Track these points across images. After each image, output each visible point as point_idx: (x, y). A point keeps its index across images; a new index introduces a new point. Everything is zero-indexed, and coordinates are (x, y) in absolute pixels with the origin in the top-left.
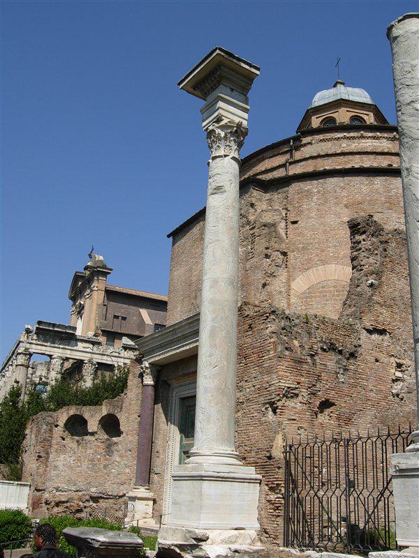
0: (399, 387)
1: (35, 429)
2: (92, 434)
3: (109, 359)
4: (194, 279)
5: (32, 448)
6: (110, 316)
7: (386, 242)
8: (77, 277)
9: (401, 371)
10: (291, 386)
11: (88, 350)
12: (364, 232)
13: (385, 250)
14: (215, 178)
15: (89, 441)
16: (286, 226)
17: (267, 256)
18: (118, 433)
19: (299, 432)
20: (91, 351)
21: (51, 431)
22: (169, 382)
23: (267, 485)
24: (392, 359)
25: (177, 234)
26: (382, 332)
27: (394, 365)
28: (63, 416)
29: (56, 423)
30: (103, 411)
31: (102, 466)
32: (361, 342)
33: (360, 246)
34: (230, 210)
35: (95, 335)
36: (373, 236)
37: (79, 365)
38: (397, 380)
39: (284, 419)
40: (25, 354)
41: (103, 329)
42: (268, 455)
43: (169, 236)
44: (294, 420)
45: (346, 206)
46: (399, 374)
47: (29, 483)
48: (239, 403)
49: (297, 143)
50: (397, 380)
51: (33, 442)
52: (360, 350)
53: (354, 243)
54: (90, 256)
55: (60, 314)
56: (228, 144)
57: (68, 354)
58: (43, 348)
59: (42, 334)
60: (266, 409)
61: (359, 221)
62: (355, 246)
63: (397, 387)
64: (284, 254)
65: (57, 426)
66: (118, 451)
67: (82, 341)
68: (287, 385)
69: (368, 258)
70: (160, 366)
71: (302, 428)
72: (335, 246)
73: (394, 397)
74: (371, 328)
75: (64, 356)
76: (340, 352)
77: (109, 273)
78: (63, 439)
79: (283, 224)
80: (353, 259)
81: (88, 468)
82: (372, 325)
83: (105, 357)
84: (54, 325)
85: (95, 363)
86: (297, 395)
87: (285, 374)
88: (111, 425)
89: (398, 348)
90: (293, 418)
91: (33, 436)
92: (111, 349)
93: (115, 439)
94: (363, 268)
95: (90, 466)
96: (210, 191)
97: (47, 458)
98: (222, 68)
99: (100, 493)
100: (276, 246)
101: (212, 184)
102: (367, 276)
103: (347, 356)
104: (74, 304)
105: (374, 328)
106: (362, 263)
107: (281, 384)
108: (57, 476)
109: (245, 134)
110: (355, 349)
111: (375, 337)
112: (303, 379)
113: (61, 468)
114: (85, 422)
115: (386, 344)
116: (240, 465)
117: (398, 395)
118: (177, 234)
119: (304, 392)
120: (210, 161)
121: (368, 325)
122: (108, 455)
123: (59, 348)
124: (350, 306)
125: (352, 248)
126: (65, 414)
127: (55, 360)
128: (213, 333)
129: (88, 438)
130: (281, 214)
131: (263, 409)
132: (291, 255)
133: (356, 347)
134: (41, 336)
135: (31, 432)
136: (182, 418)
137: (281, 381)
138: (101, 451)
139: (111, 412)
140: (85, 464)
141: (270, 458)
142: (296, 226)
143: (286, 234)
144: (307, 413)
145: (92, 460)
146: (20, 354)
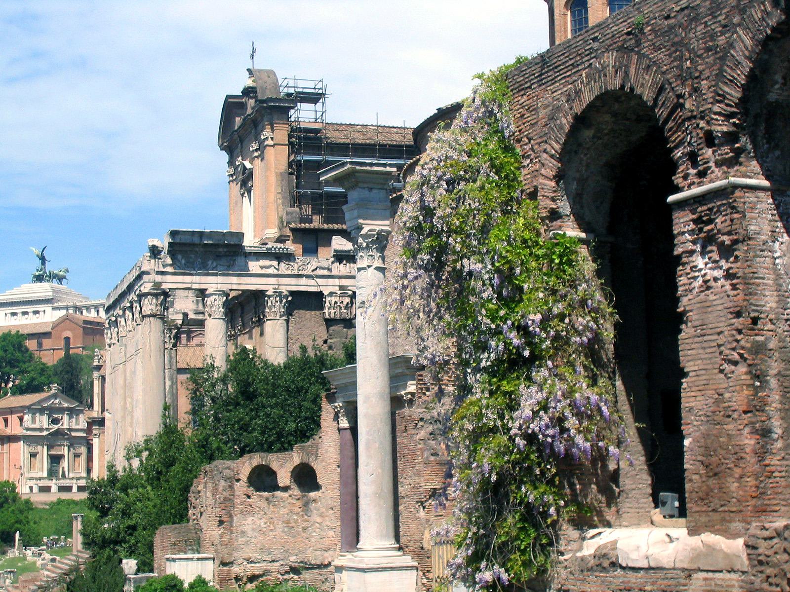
1: (210, 485)
2: (286, 489)
3: (311, 282)
5: (209, 509)
8: (231, 107)
11: (271, 271)
15: (282, 499)
18: (317, 487)
20: (276, 272)
21: (231, 487)
23: (421, 570)
28: (245, 466)
29: (237, 477)
30: (295, 459)
31: (301, 529)
34: (377, 325)
40: (156, 296)
41: (293, 226)
47: (212, 556)
51: (210, 501)
56: (370, 253)
57: (235, 283)
58: (188, 279)
59: (181, 252)
65: (238, 480)
66: (318, 510)
67: (258, 256)
68: (432, 487)
78: (249, 497)
81: (283, 532)
83: (304, 281)
84: (201, 234)
85: (286, 293)
88: (306, 478)
91: (209, 494)
92: (313, 263)
93: (312, 495)
95: (286, 529)
97: (231, 522)
99: (302, 562)
104: (231, 163)
108: (247, 543)
113: (250, 533)
114: (273, 474)
116: (400, 556)
122: (306, 515)
123: (216, 275)
126: (247, 464)
127: (212, 298)
129: (278, 493)
131: (417, 506)
134: (179, 257)
135: (205, 487)
138: (297, 509)
139: (305, 460)
140: (280, 526)
141: (422, 548)
145: (288, 522)
146: (146, 295)
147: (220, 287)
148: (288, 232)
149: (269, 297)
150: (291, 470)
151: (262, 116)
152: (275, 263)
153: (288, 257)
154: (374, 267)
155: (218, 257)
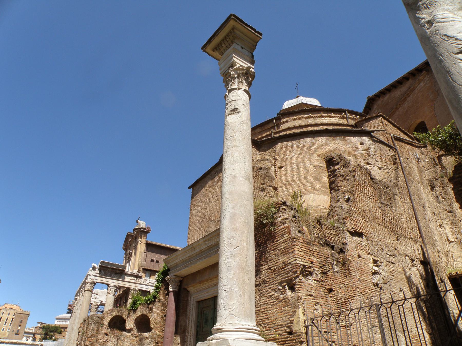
0: (378, 279)
2: (130, 330)
4: (207, 214)
6: (149, 260)
7: (354, 171)
8: (128, 236)
9: (377, 266)
10: (306, 264)
11: (133, 281)
12: (338, 164)
13: (354, 177)
14: (231, 103)
16: (275, 170)
17: (263, 190)
19: (316, 307)
21: (98, 328)
22: (188, 289)
24: (370, 257)
25: (196, 187)
26: (360, 235)
27: (372, 260)
32: (346, 241)
33: (336, 173)
34: (244, 125)
35: (139, 271)
36: (344, 167)
37: (127, 291)
38: (375, 273)
39: (302, 294)
40: (91, 283)
42: (288, 330)
43: (189, 188)
44: (311, 296)
45: (318, 155)
46: (376, 268)
48: (257, 285)
49: (278, 121)
50: (375, 273)
52: (347, 247)
53: (331, 172)
54: (137, 222)
55: (116, 259)
57: (120, 283)
58: (104, 279)
59: (103, 270)
60: (284, 287)
61: (334, 155)
62: (332, 175)
63: (376, 279)
64: (275, 189)
67: (130, 275)
69: (342, 181)
70: (182, 277)
71: (318, 303)
72: (312, 182)
73: (375, 286)
74: (353, 230)
75: (117, 285)
76: (333, 248)
77: (149, 232)
78: (107, 335)
79: (273, 169)
80: (331, 183)
82: (353, 228)
83: (144, 286)
86: (311, 274)
87: (300, 253)
89: (373, 248)
90: (310, 293)
94: (340, 188)
96: (227, 112)
98: (235, 30)
100: (269, 183)
101: (230, 107)
102: (344, 193)
103: (338, 251)
105: (354, 231)
106: (339, 185)
107: (298, 262)
109: (253, 76)
110: (343, 246)
111: (355, 238)
112: (315, 259)
114: (124, 321)
115: (364, 244)
116: (262, 341)
117: (377, 285)
118: (196, 187)
119: (318, 271)
120: (227, 94)
121: (350, 228)
123: (114, 279)
124: (333, 216)
125: (329, 176)
127: (111, 288)
128: (233, 218)
129: (125, 333)
130: (271, 162)
132: (280, 190)
133: (343, 244)
134: (102, 271)
136: (198, 317)
137: (298, 259)
141: (290, 333)
142: (283, 169)
143: (276, 175)
144: (321, 290)
146: (87, 283)
147: (114, 284)
148: (141, 269)
149: (131, 290)
150: (135, 319)
151: (139, 234)
152: (135, 279)
153: (140, 277)
154: (243, 89)
155: (116, 273)
